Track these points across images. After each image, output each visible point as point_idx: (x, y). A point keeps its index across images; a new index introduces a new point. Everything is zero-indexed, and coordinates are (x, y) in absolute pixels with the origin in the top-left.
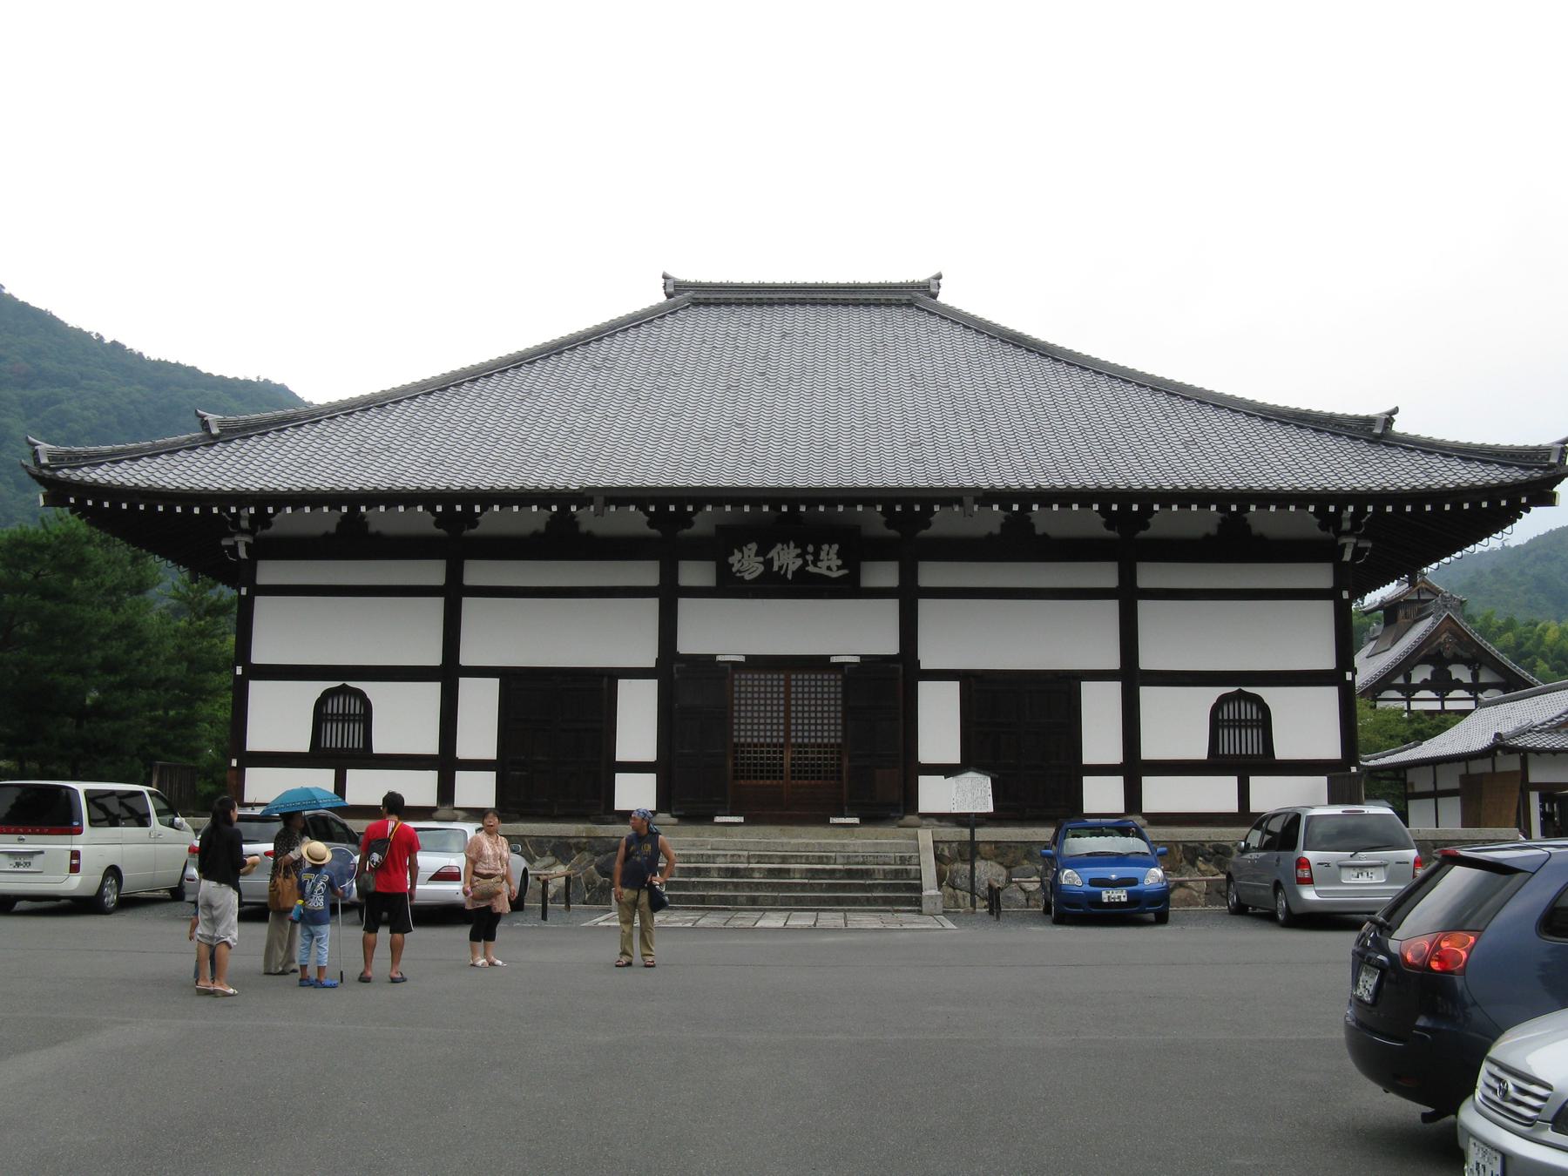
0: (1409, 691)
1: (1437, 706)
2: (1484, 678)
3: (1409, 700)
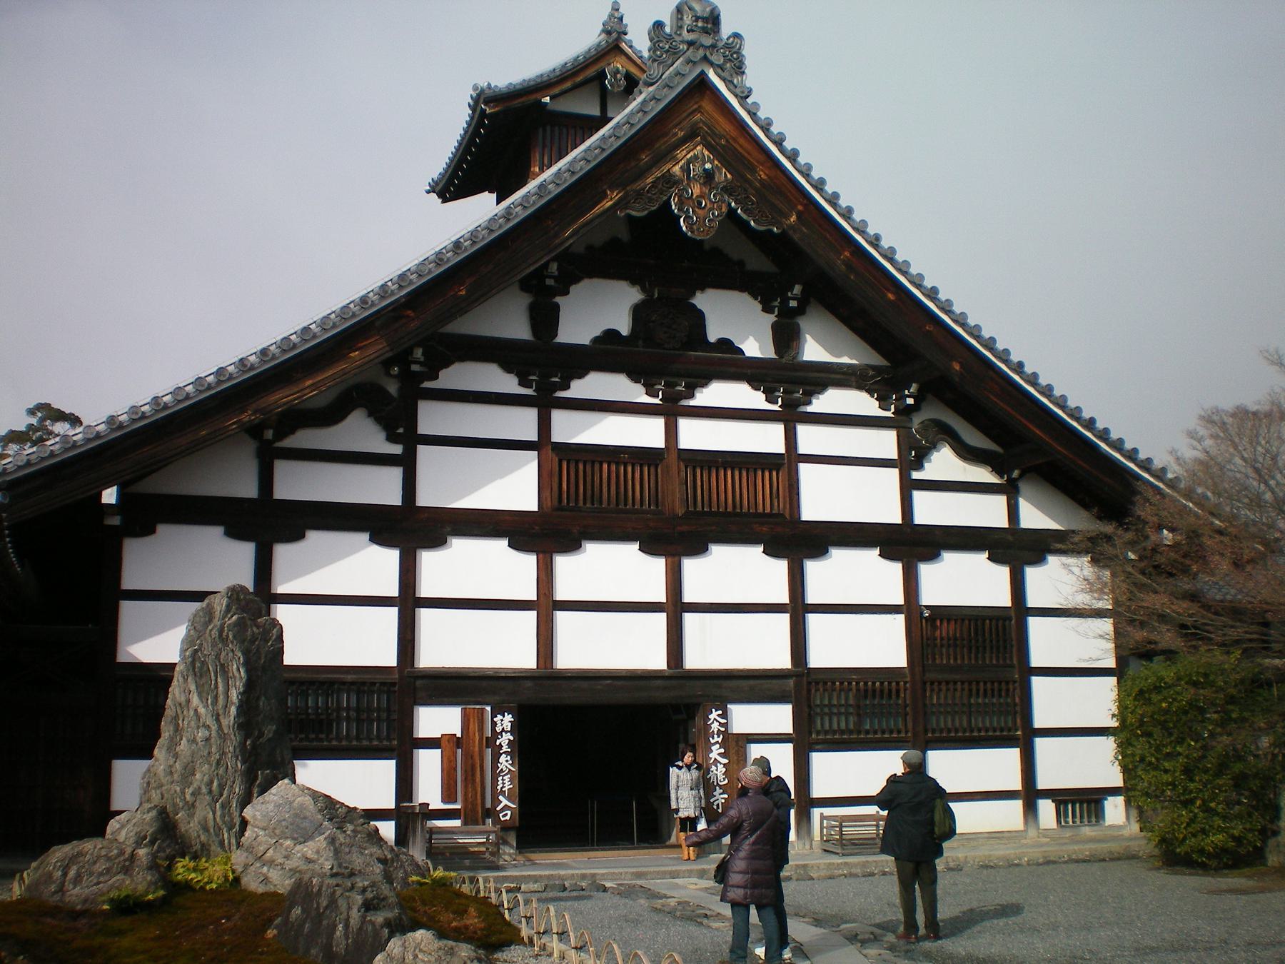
0: (546, 371)
1: (645, 433)
3: (546, 403)
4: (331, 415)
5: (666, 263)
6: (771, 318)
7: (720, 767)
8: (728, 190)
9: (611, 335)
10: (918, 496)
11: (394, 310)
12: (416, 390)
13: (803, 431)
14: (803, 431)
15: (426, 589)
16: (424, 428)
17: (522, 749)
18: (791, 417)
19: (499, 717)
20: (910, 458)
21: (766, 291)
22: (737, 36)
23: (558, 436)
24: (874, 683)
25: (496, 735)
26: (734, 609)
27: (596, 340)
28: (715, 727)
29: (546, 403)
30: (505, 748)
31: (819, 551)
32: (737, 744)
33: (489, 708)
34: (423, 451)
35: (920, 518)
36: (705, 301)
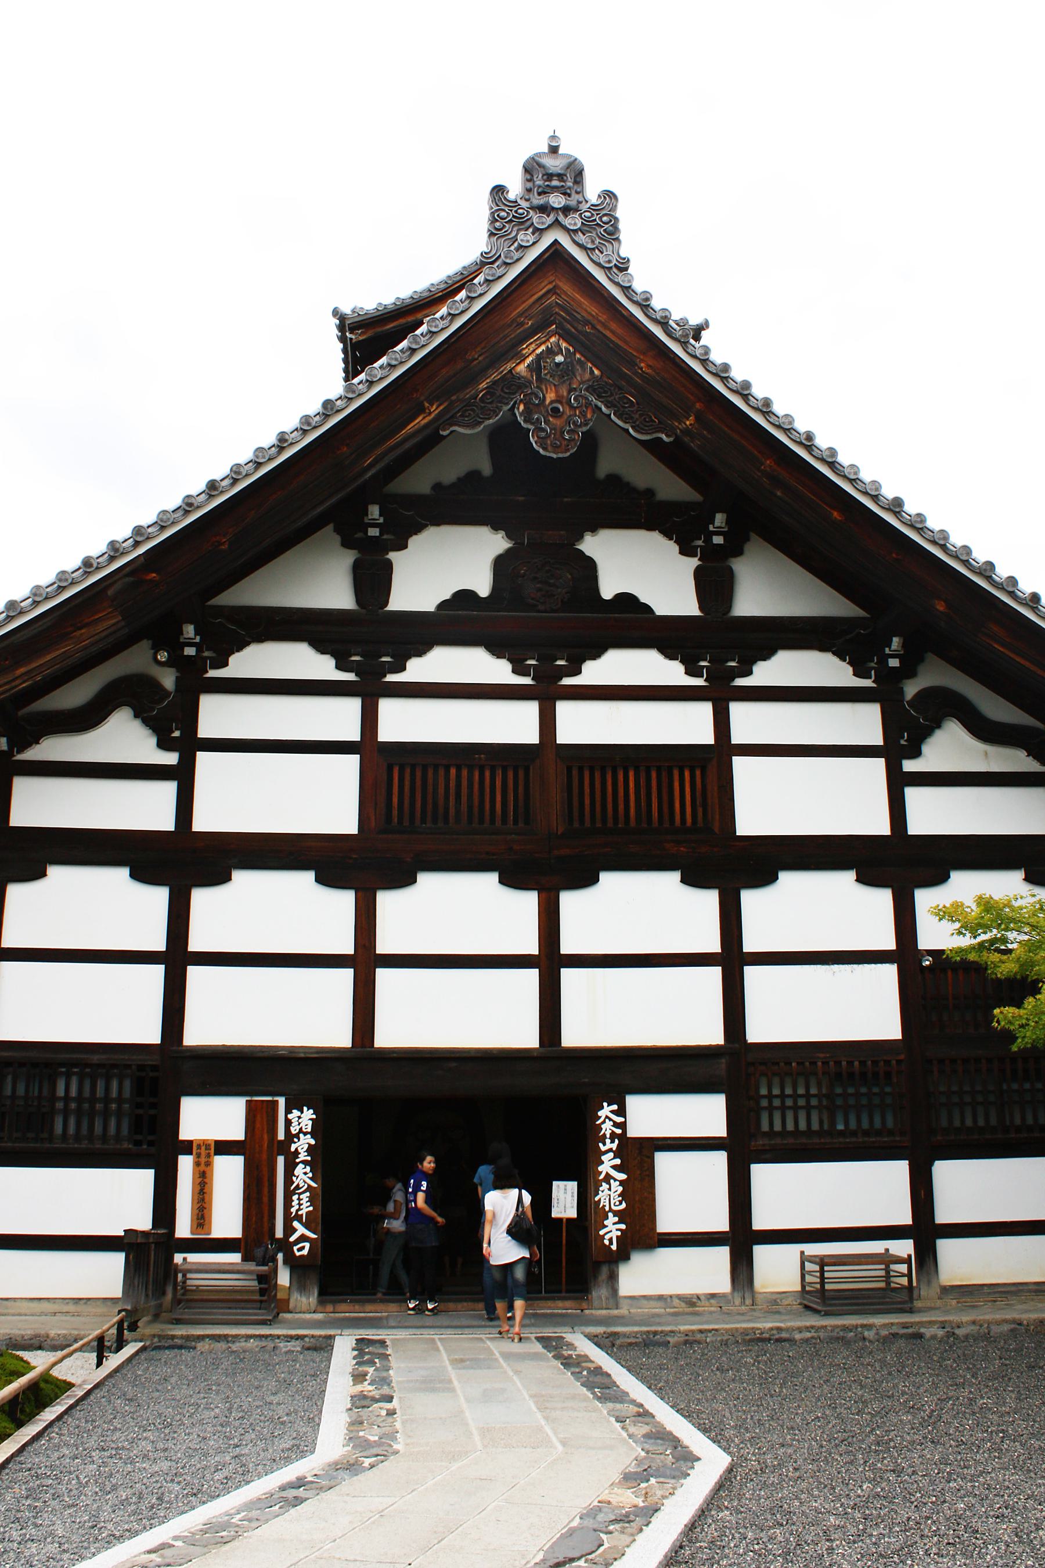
0: (371, 647)
1: (515, 724)
2: (762, 591)
3: (370, 690)
4: (87, 719)
5: (549, 507)
6: (694, 562)
7: (615, 1185)
8: (596, 388)
9: (464, 598)
10: (913, 795)
11: (132, 573)
12: (196, 684)
13: (738, 710)
14: (738, 710)
15: (200, 938)
16: (205, 731)
17: (321, 1158)
18: (720, 694)
19: (296, 1113)
20: (898, 746)
21: (681, 527)
22: (609, 195)
23: (387, 733)
24: (850, 1063)
25: (290, 1137)
26: (639, 960)
27: (443, 605)
28: (607, 1128)
29: (370, 690)
30: (303, 1156)
31: (765, 878)
32: (640, 1155)
33: (282, 1101)
34: (203, 758)
35: (916, 826)
36: (591, 545)
